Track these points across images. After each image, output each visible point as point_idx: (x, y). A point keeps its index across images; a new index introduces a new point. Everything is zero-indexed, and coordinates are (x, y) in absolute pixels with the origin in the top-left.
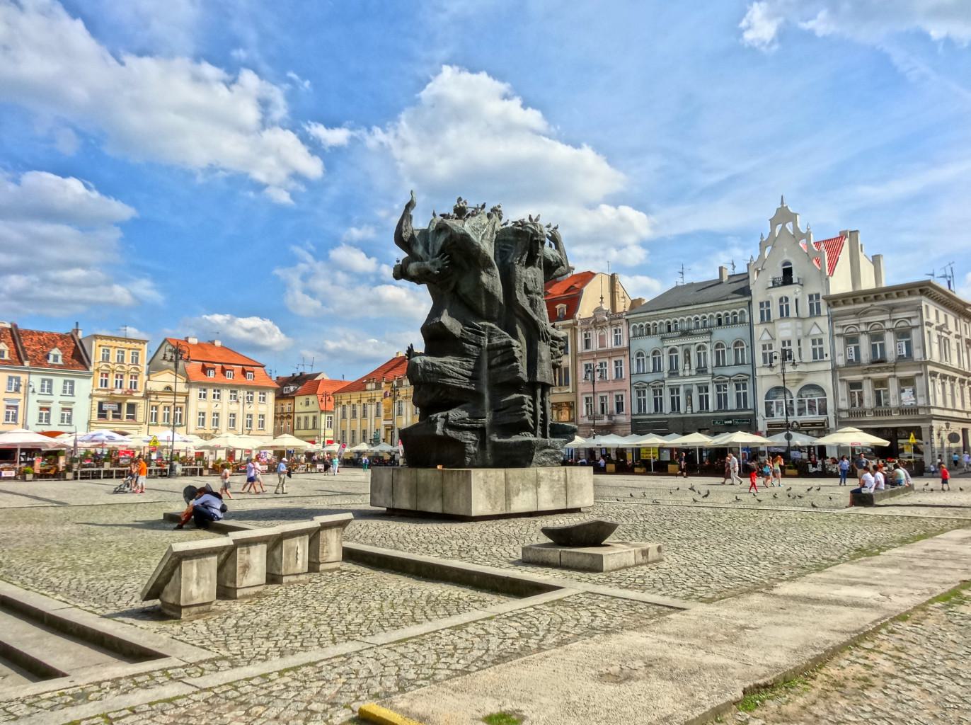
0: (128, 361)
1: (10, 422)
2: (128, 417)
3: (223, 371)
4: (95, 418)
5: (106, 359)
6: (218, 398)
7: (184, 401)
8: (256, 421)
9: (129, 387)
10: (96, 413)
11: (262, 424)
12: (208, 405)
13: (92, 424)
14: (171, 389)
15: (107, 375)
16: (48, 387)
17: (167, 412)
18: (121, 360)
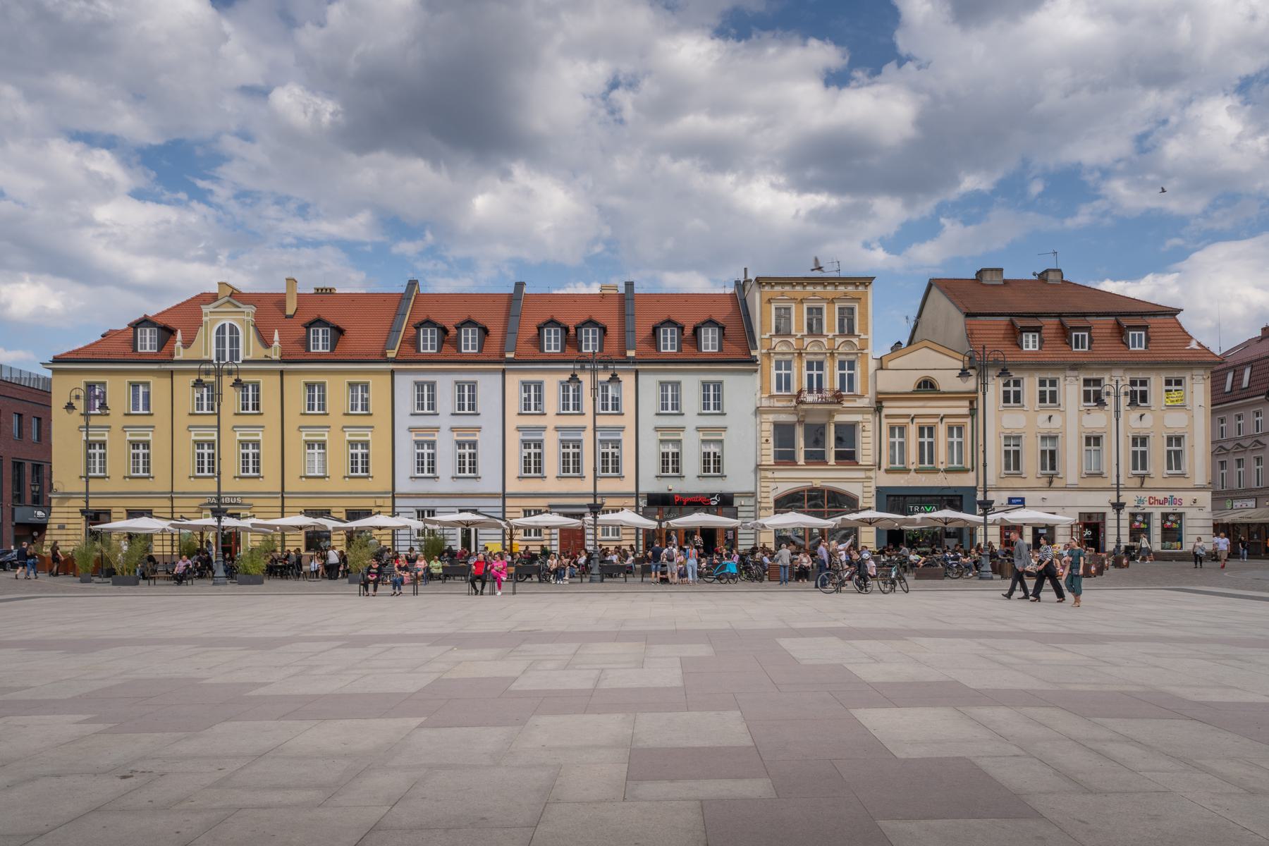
0: (831, 328)
1: (571, 473)
2: (840, 456)
3: (1065, 333)
4: (770, 460)
5: (782, 331)
6: (1053, 400)
7: (966, 411)
8: (1157, 452)
9: (837, 386)
10: (770, 449)
11: (1175, 459)
12: (1027, 421)
13: (764, 474)
14: (932, 386)
15: (820, 366)
16: (671, 402)
17: (955, 439)
18: (814, 329)
